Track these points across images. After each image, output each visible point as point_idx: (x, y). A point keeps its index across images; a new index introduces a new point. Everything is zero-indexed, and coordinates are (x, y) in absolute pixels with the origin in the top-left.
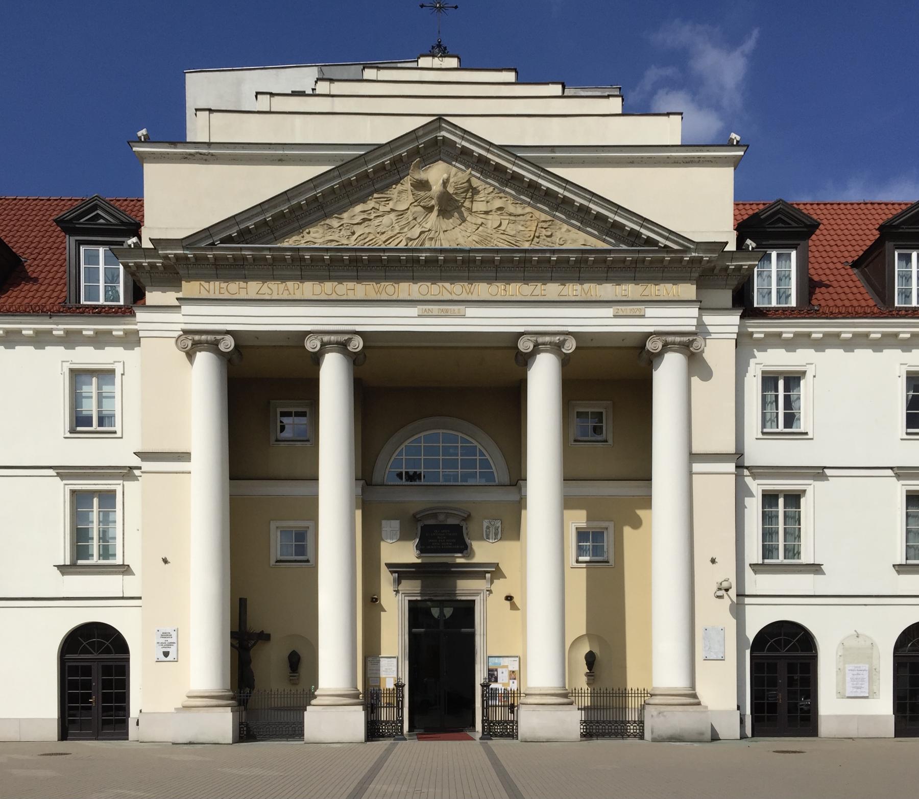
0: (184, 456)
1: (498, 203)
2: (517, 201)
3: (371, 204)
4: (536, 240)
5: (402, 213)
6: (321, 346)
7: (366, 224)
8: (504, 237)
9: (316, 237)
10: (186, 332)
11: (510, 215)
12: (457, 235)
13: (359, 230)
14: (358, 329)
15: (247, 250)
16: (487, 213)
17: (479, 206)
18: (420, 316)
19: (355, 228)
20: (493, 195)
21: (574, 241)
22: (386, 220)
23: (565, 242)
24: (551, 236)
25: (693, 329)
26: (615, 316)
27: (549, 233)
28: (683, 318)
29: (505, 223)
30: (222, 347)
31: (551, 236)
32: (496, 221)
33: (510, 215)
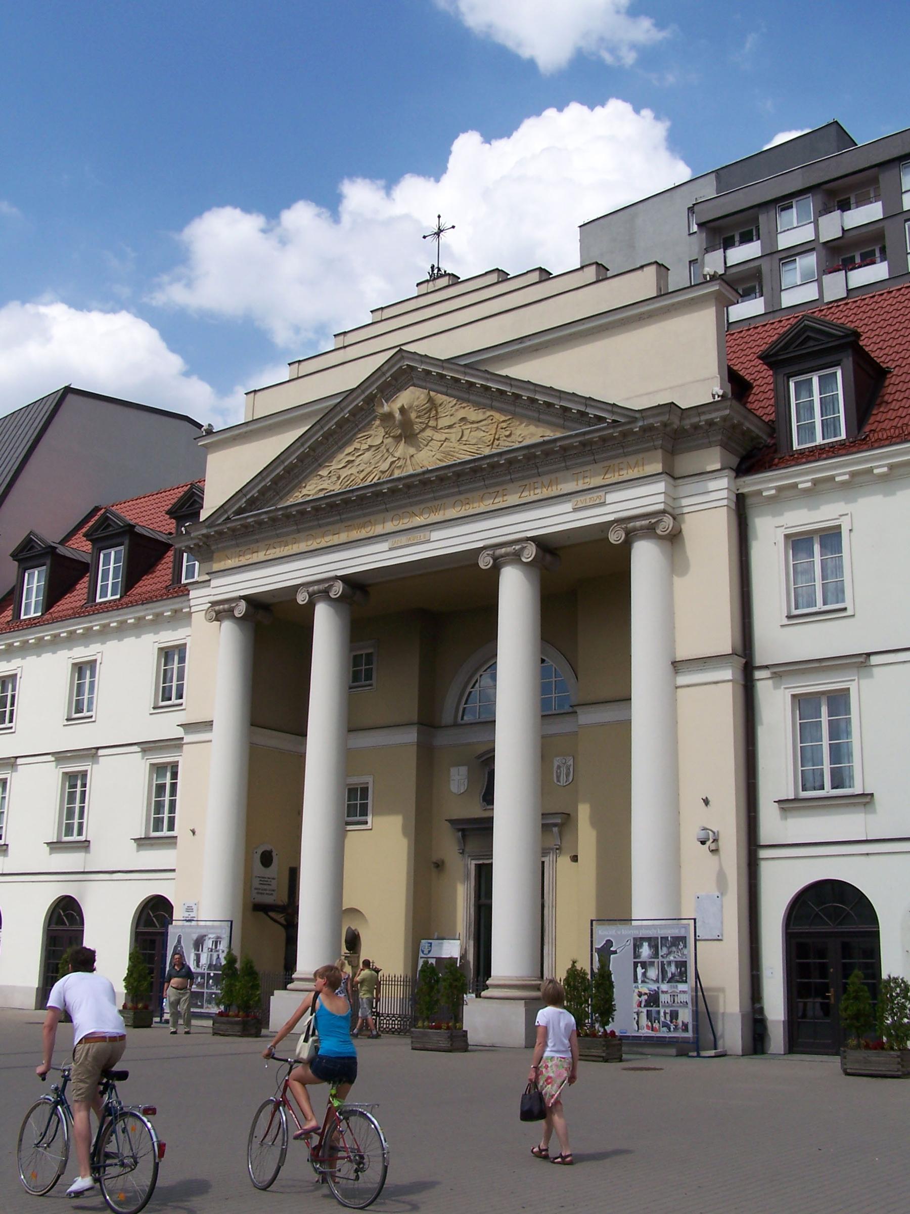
0: (208, 725)
1: (461, 414)
2: (479, 406)
3: (356, 445)
4: (496, 442)
5: (378, 447)
6: (310, 597)
7: (349, 466)
8: (465, 447)
9: (312, 489)
10: (214, 604)
11: (473, 423)
12: (426, 458)
13: (344, 473)
14: (340, 573)
15: (249, 518)
16: (450, 427)
17: (443, 422)
18: (390, 549)
19: (341, 472)
20: (456, 407)
21: (532, 435)
22: (368, 455)
23: (524, 438)
24: (510, 435)
25: (661, 507)
26: (575, 510)
27: (507, 433)
28: (644, 497)
29: (467, 432)
30: (237, 614)
31: (510, 435)
32: (461, 434)
33: (473, 423)
